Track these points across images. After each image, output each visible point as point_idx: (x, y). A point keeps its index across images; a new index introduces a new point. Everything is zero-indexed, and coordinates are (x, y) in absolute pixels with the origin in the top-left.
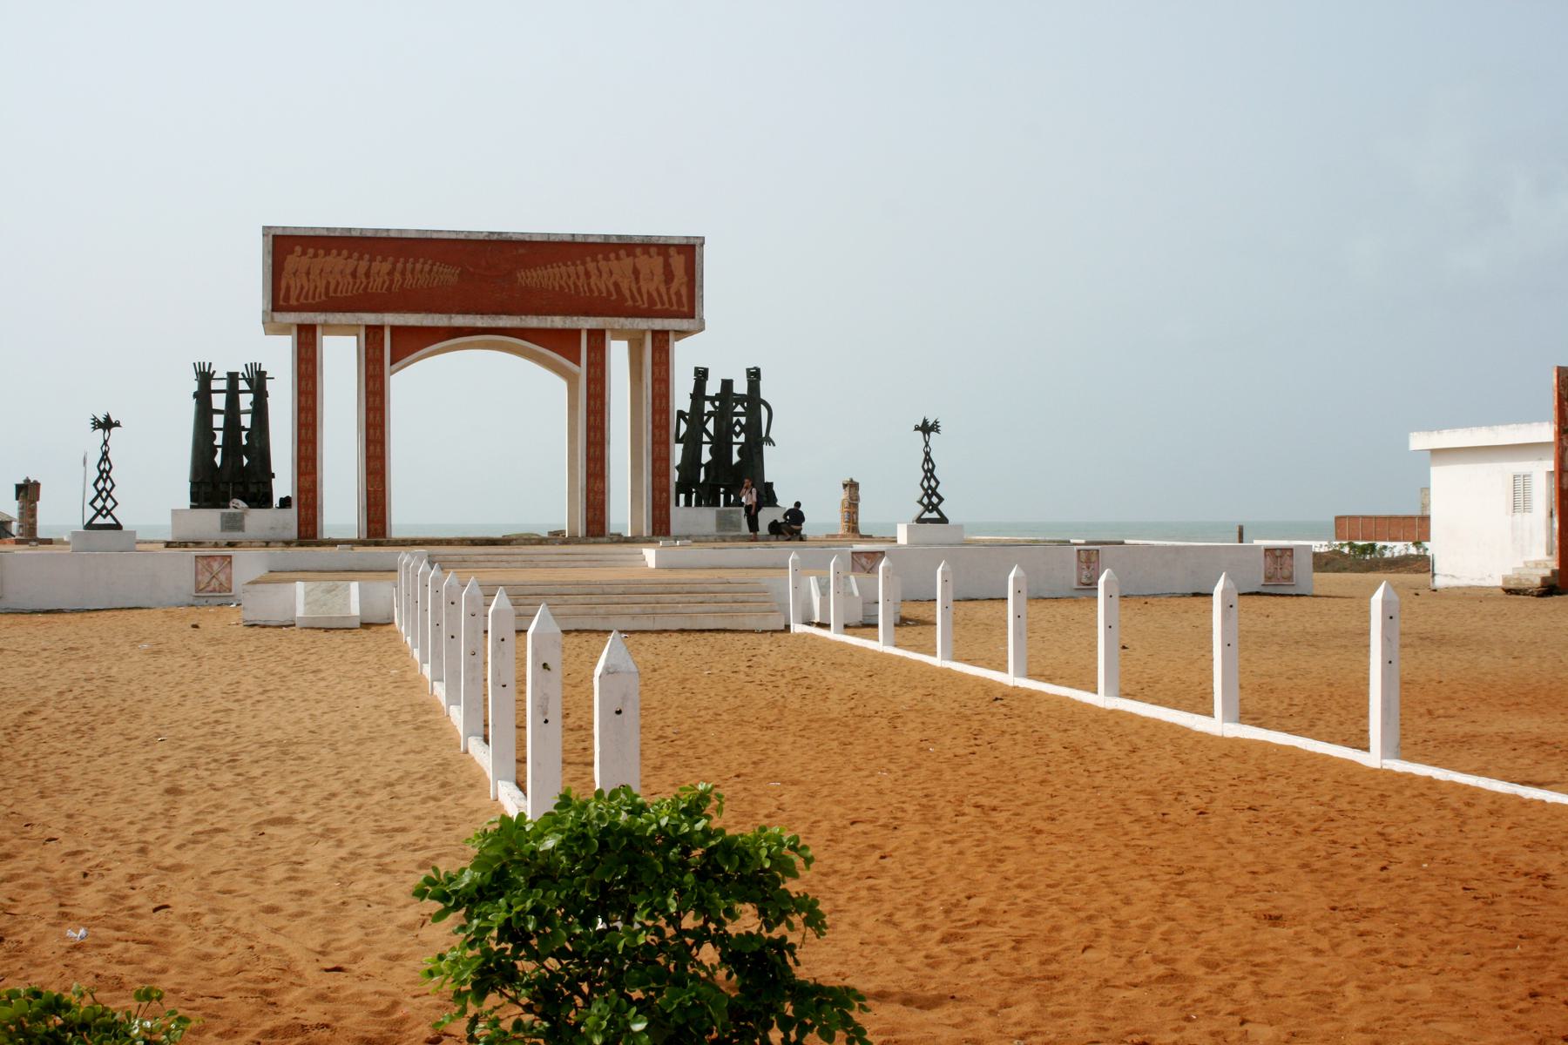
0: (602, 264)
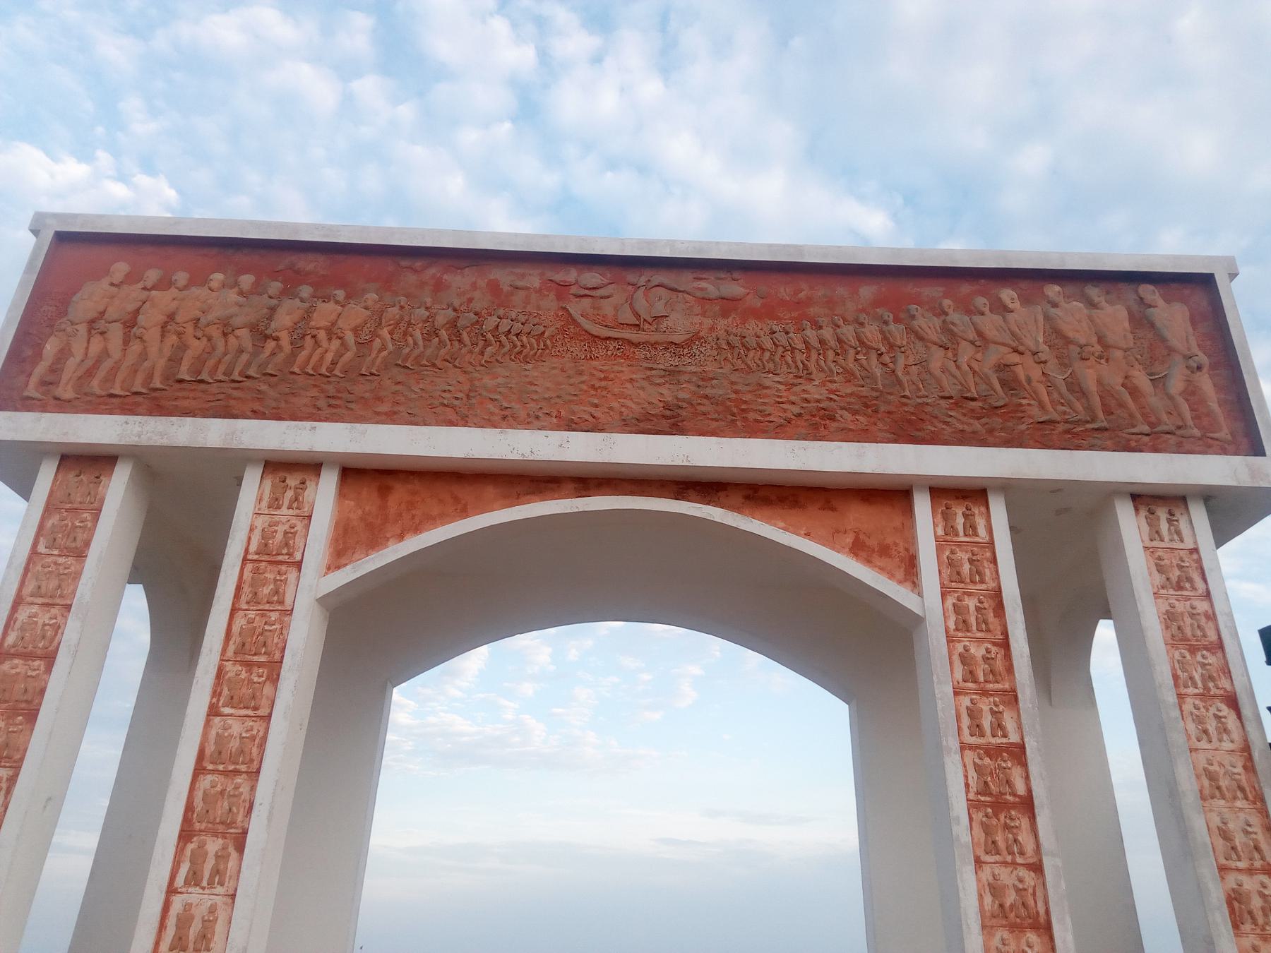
0: (955, 317)
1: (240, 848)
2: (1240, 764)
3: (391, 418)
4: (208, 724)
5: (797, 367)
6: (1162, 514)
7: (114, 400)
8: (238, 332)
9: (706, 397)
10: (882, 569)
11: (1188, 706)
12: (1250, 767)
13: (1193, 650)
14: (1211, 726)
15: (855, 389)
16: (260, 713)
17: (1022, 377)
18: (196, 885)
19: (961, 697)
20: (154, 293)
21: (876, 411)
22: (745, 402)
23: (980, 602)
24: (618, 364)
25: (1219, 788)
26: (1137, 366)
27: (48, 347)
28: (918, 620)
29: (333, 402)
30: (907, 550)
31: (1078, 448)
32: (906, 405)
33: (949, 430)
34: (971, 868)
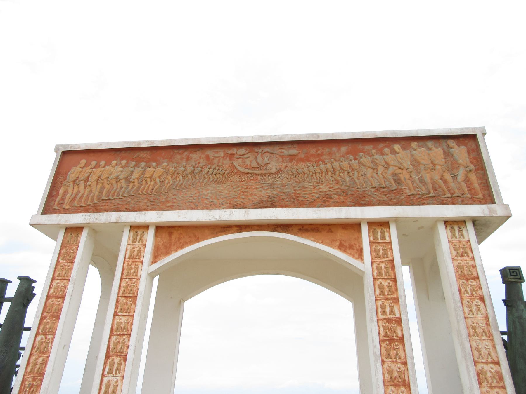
0: (377, 156)
1: (125, 361)
2: (485, 323)
3: (172, 208)
4: (114, 318)
5: (317, 179)
6: (456, 228)
7: (82, 208)
8: (121, 181)
9: (284, 193)
10: (350, 254)
11: (465, 301)
12: (488, 324)
13: (467, 280)
14: (474, 309)
15: (339, 186)
16: (130, 314)
17: (402, 179)
18: (111, 373)
19: (378, 301)
20: (94, 169)
21: (347, 195)
22: (298, 194)
23: (386, 265)
24: (252, 183)
25: (475, 332)
26: (446, 171)
27: (61, 191)
28: (363, 272)
29: (152, 203)
30: (359, 246)
31: (423, 204)
32: (358, 191)
33: (375, 200)
34: (379, 364)
